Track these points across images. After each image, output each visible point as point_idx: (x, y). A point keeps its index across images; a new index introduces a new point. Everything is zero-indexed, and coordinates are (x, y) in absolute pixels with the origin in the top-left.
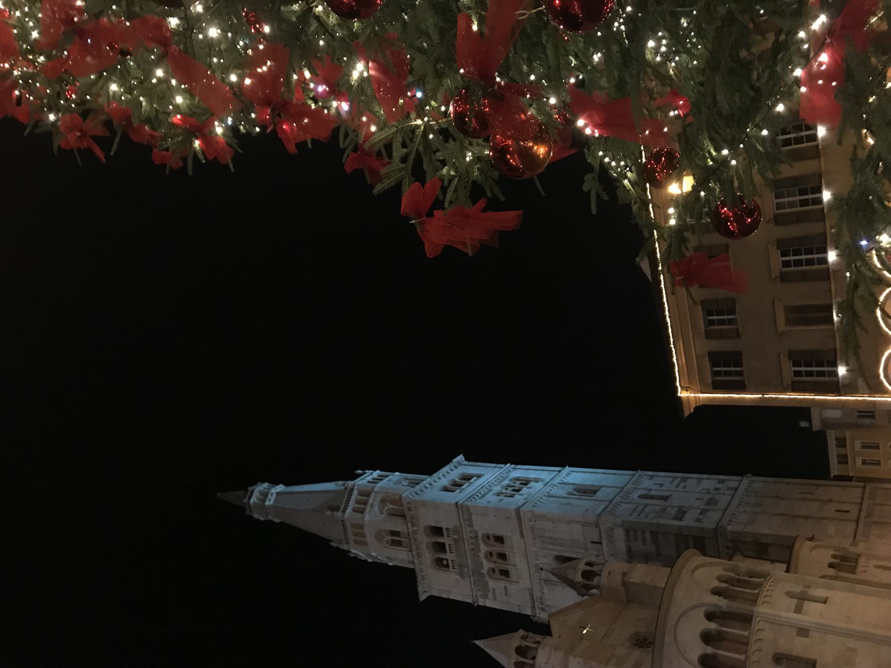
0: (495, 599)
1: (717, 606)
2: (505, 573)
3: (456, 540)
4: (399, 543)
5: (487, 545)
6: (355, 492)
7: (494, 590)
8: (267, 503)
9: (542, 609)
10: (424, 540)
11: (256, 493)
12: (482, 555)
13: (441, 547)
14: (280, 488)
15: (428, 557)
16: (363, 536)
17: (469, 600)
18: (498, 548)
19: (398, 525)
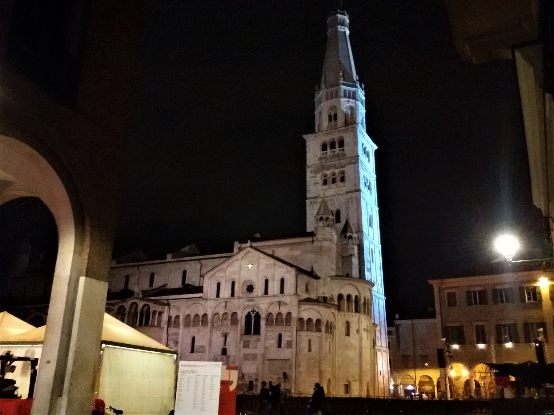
0: (312, 177)
1: (360, 300)
2: (325, 183)
3: (338, 155)
4: (330, 120)
5: (339, 173)
6: (354, 89)
7: (315, 177)
8: (339, 27)
9: (311, 203)
10: (336, 136)
11: (343, 17)
12: (333, 170)
13: (333, 146)
14: (348, 33)
15: (327, 139)
16: (332, 98)
17: (308, 163)
18: (338, 178)
19: (341, 120)
